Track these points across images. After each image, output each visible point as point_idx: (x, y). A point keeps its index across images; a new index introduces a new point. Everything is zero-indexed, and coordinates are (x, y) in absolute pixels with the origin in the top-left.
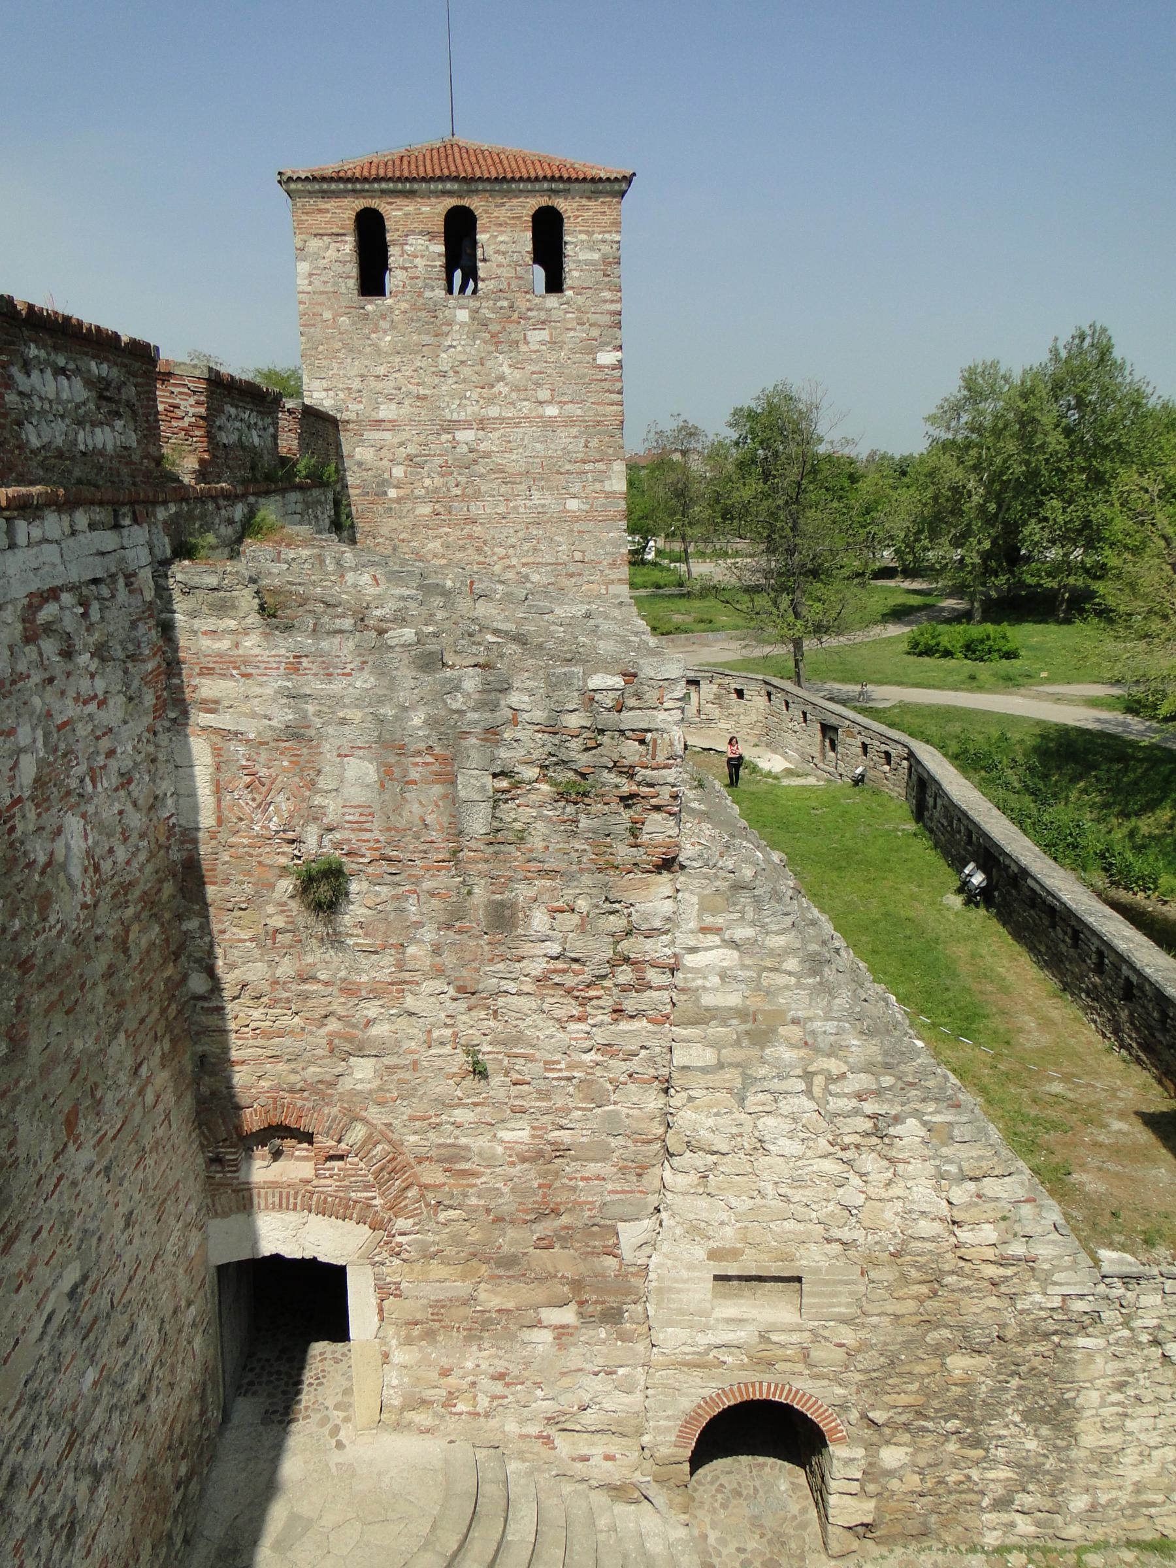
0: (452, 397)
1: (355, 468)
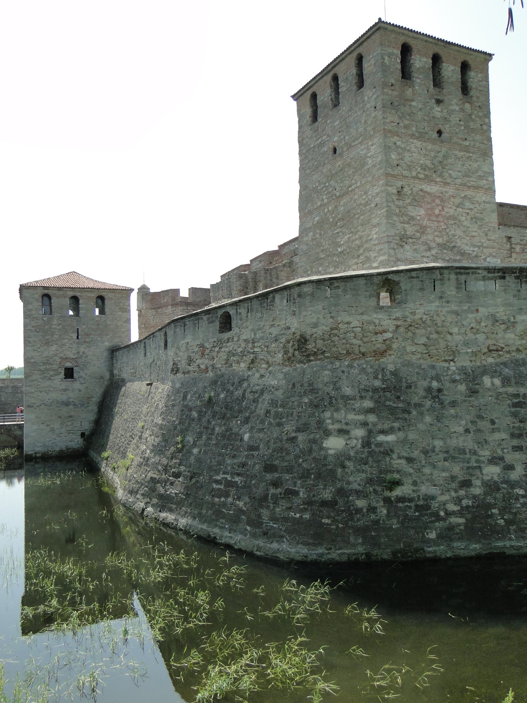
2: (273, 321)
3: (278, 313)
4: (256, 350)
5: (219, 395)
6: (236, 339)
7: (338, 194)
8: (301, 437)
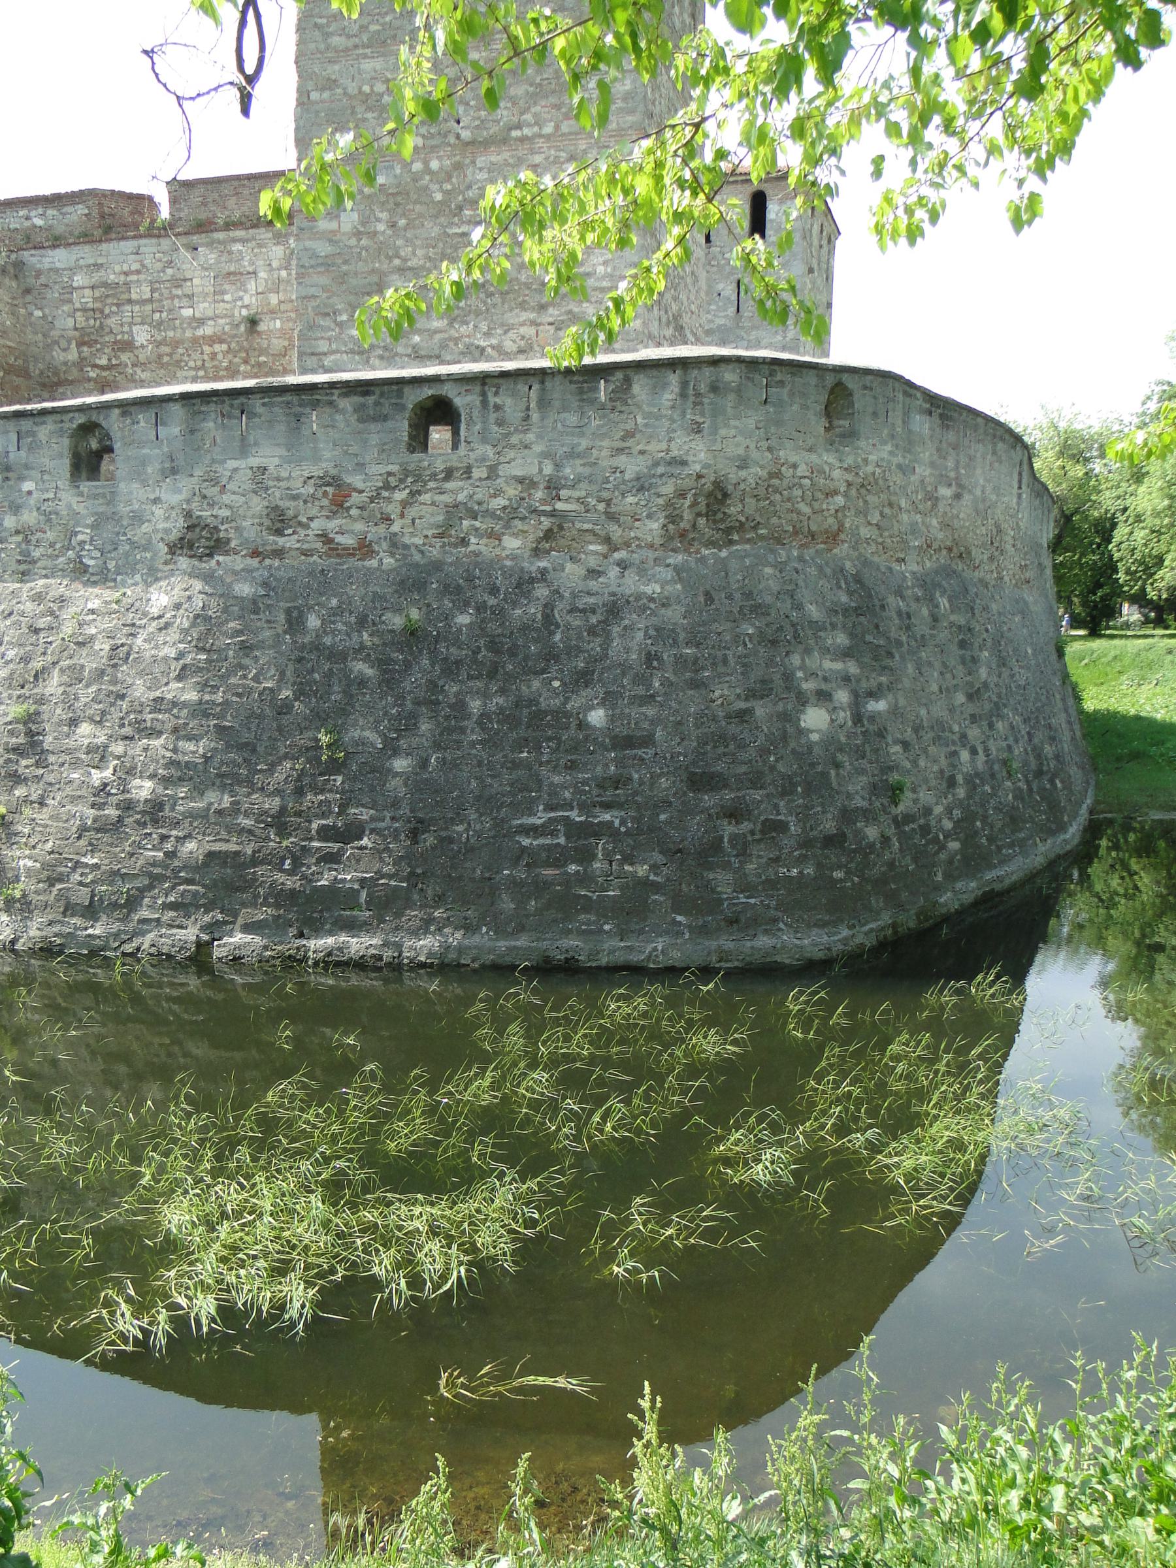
2: (623, 439)
3: (639, 420)
4: (560, 506)
5: (447, 618)
6: (478, 473)
7: (466, 135)
8: (761, 710)
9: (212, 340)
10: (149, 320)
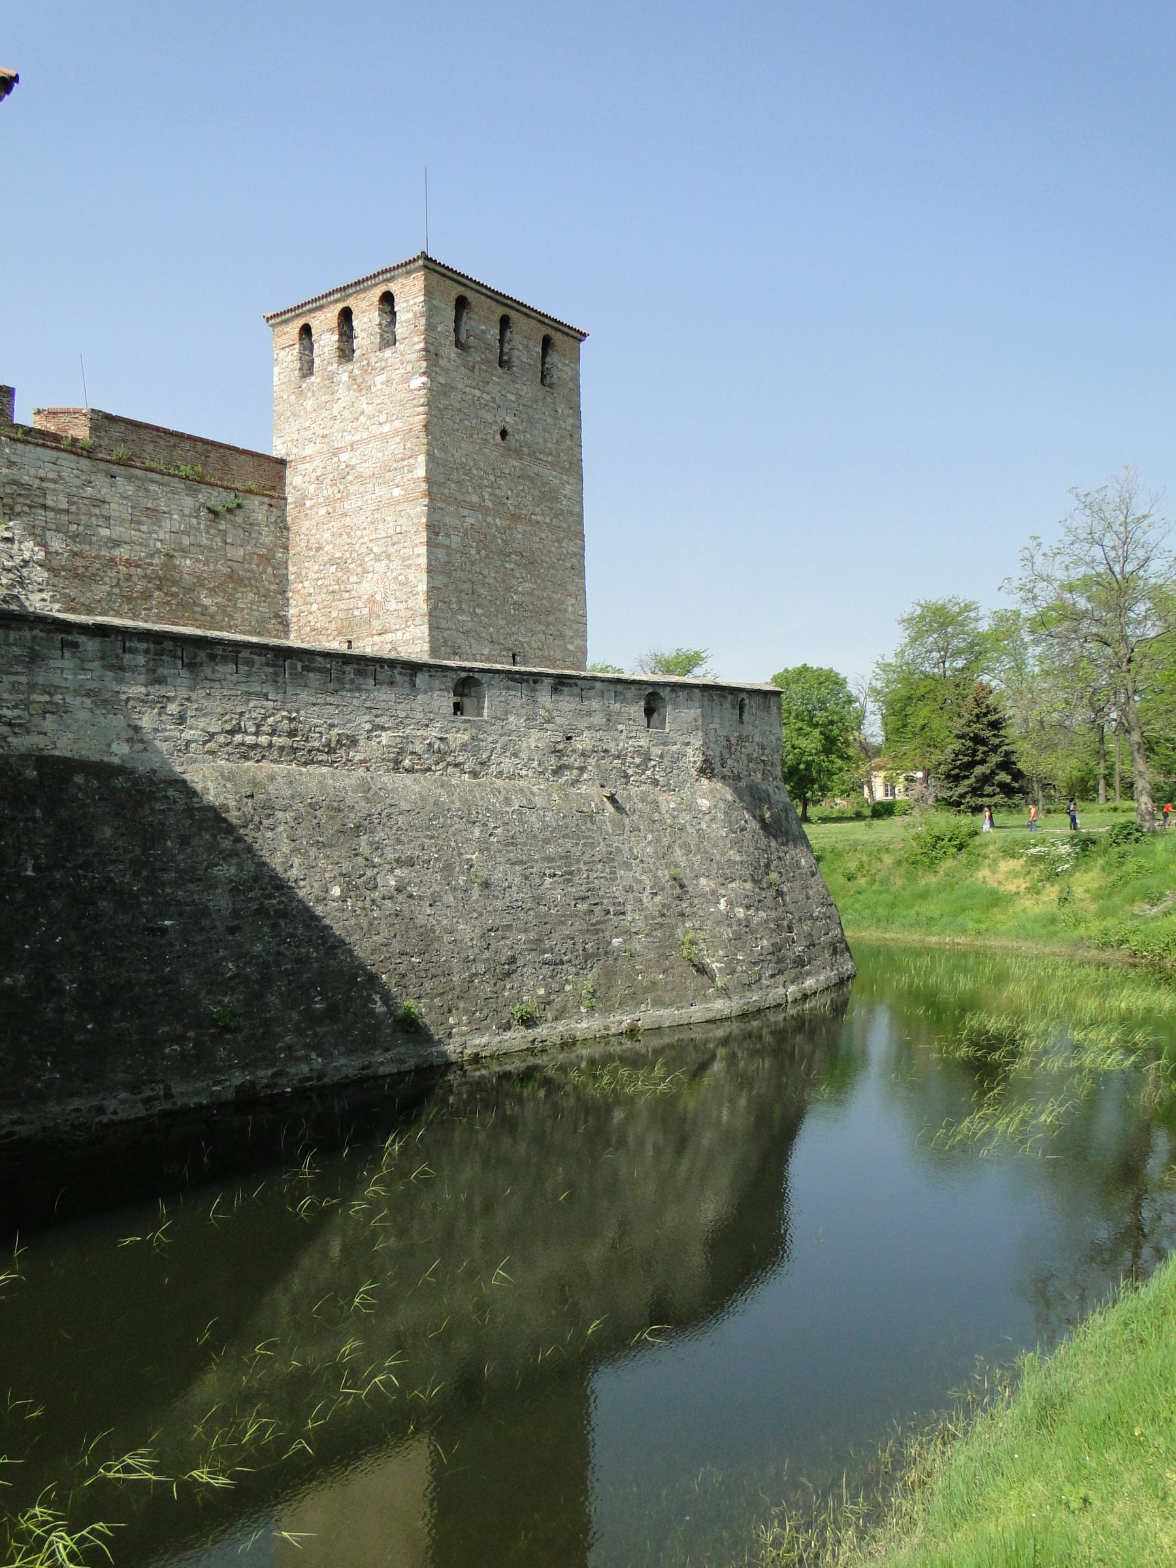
0: (338, 432)
1: (293, 491)
7: (512, 508)
9: (128, 563)
10: (64, 529)
